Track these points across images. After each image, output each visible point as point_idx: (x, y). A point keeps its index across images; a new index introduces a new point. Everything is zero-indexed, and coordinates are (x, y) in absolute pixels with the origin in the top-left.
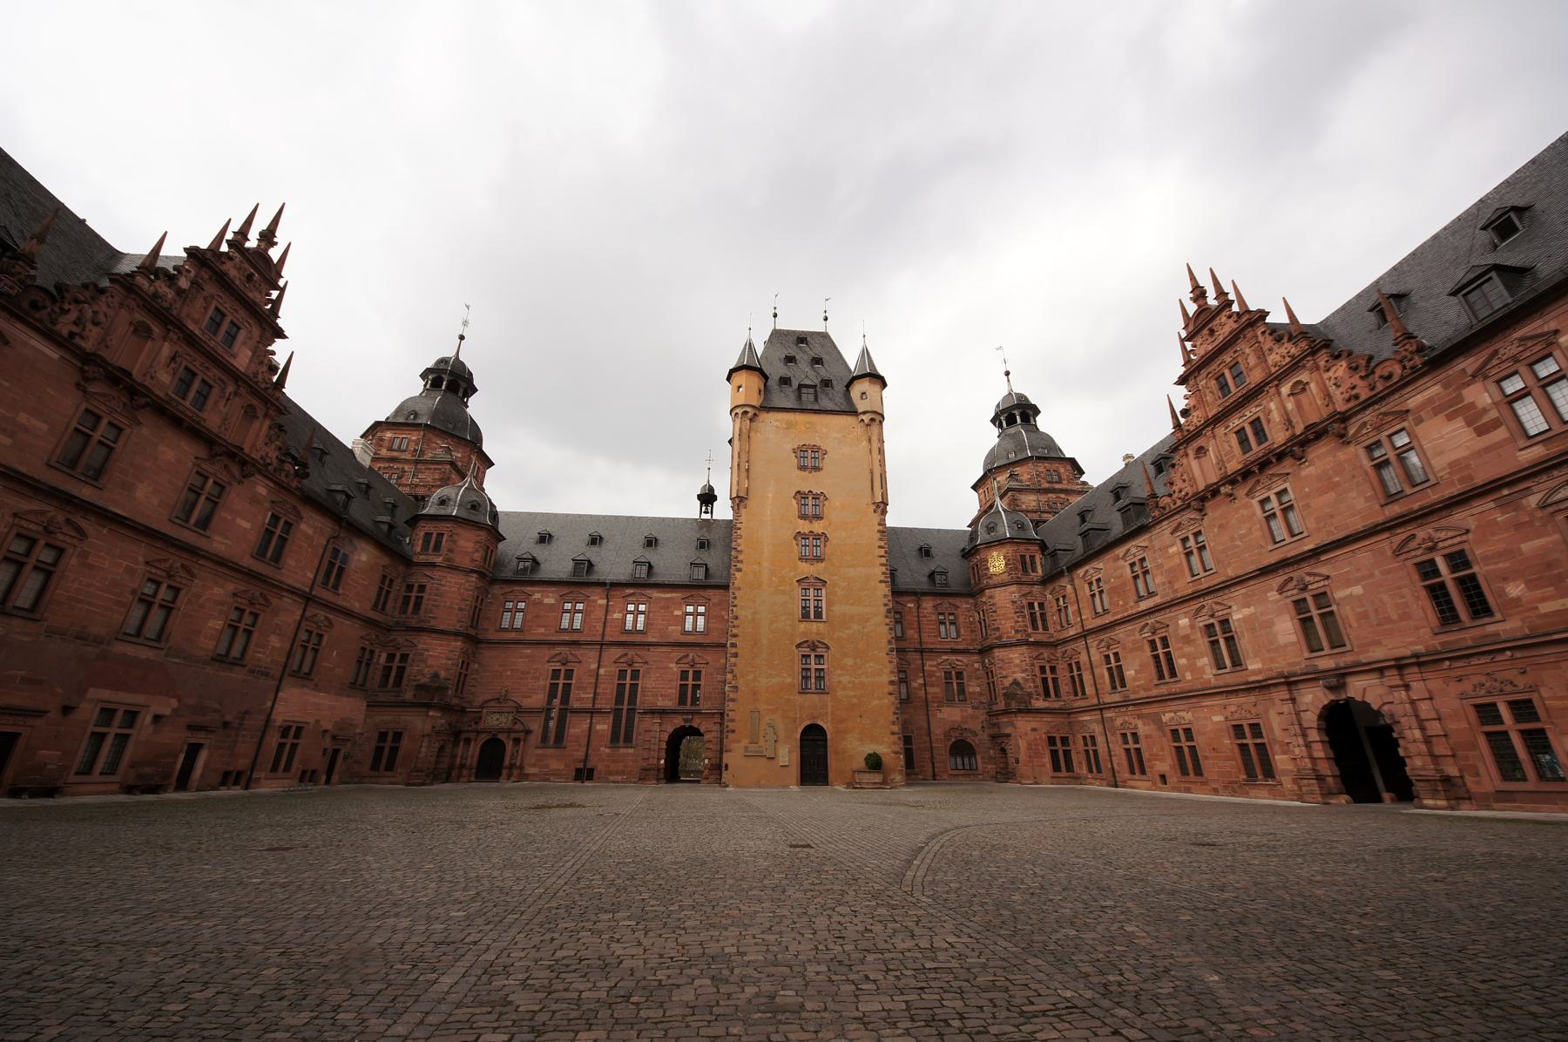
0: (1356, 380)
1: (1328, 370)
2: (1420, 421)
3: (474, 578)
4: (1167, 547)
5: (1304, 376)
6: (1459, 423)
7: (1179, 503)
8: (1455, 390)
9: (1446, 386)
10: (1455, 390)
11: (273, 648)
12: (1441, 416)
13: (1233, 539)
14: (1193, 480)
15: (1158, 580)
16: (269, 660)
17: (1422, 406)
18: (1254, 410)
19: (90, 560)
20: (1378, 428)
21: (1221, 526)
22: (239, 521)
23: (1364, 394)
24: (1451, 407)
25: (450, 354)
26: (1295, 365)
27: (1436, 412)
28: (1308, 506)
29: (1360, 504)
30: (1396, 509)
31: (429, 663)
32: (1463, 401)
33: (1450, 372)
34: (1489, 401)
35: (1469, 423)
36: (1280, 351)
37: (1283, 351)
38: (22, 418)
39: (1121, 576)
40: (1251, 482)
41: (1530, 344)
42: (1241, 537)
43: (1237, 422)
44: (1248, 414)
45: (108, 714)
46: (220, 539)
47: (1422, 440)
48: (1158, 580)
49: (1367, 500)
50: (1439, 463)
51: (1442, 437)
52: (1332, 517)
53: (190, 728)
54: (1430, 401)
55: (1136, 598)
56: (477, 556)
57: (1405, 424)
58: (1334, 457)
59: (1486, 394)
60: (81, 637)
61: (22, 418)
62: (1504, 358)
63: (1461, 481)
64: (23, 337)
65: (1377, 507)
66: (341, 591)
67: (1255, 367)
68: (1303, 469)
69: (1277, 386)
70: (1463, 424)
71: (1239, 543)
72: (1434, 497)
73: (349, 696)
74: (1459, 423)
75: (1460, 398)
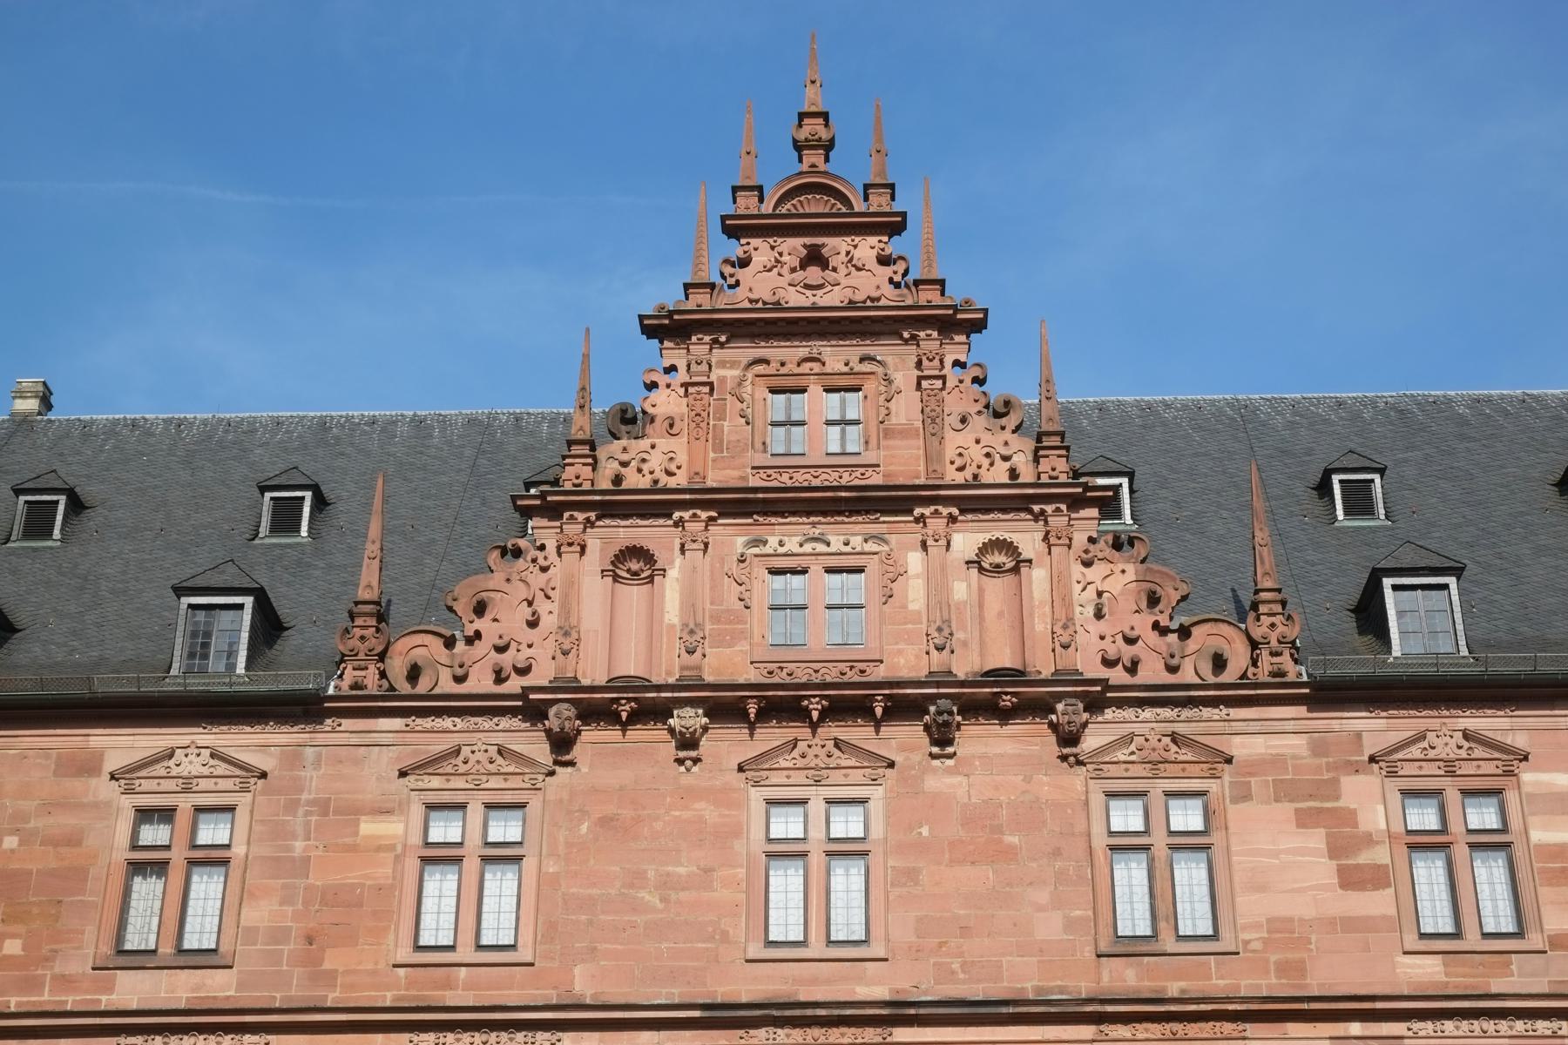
0: (1142, 624)
1: (1087, 564)
2: (1243, 795)
4: (356, 811)
5: (1027, 539)
6: (1316, 839)
7: (479, 682)
8: (1329, 767)
9: (1318, 749)
10: (1329, 767)
12: (1287, 809)
13: (636, 879)
14: (568, 633)
15: (257, 914)
17: (1257, 766)
18: (857, 541)
20: (1156, 765)
21: (605, 822)
23: (1154, 671)
24: (1311, 797)
26: (1016, 503)
27: (1283, 792)
28: (911, 875)
29: (1049, 927)
30: (1126, 977)
32: (1337, 798)
33: (1335, 725)
34: (1383, 826)
35: (1334, 851)
36: (987, 438)
37: (996, 441)
39: (73, 840)
40: (772, 735)
41: (1479, 752)
42: (666, 884)
43: (792, 545)
44: (836, 544)
47: (1233, 840)
48: (257, 914)
49: (1070, 925)
50: (1251, 908)
51: (1276, 854)
52: (965, 931)
54: (1277, 762)
55: (106, 949)
57: (1212, 786)
58: (1028, 780)
59: (1381, 808)
62: (1432, 754)
63: (1283, 968)
65: (1089, 953)
67: (905, 433)
68: (935, 770)
69: (952, 519)
70: (1323, 846)
71: (650, 897)
72: (1219, 980)
74: (1316, 839)
75: (1331, 789)
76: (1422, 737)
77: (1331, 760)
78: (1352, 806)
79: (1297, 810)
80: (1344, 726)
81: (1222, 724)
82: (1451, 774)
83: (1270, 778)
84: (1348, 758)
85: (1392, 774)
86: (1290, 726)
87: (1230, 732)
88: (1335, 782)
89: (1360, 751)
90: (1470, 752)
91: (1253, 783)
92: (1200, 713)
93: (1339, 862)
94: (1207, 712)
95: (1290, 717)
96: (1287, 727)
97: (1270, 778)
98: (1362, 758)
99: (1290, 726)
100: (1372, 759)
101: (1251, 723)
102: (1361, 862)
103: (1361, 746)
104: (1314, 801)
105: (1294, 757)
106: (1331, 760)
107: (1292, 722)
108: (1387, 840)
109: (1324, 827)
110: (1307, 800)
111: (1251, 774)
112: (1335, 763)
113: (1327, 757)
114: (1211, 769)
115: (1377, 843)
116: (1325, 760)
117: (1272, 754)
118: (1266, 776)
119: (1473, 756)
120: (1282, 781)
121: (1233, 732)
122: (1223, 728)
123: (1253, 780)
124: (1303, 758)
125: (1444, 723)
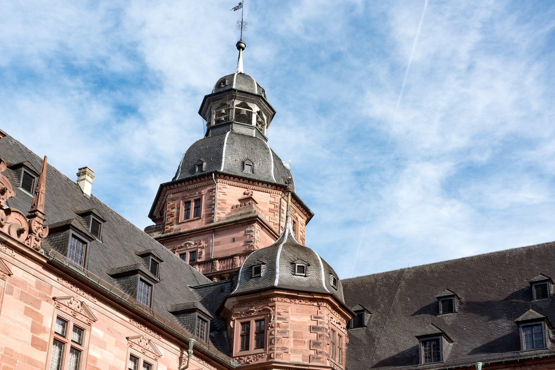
6: (28, 321)
8: (40, 295)
9: (38, 286)
10: (40, 295)
12: (22, 305)
17: (16, 282)
27: (23, 297)
34: (50, 327)
54: (24, 284)
74: (28, 321)
76: (69, 298)
77: (41, 292)
78: (43, 314)
79: (26, 307)
80: (49, 281)
81: (11, 258)
82: (74, 316)
83: (20, 290)
84: (46, 294)
85: (58, 307)
86: (33, 272)
87: (13, 263)
88: (40, 302)
89: (50, 294)
90: (81, 311)
91: (14, 289)
92: (5, 249)
93: (33, 335)
94: (9, 251)
95: (34, 268)
96: (32, 272)
97: (20, 290)
98: (50, 296)
99: (33, 272)
100: (54, 299)
101: (21, 264)
102: (40, 338)
103: (51, 291)
104: (32, 306)
105: (30, 285)
106: (41, 292)
107: (34, 271)
108: (50, 333)
109: (32, 318)
110: (30, 305)
111: (15, 285)
112: (42, 294)
113: (40, 290)
114: (3, 275)
115: (46, 332)
116: (39, 291)
117: (23, 280)
118: (19, 287)
119: (81, 313)
120: (24, 292)
121: (14, 264)
122: (11, 260)
123: (15, 287)
124: (32, 287)
125: (77, 296)
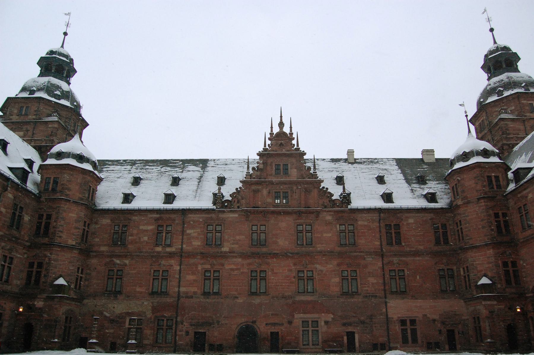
3: (482, 203)
11: (373, 284)
16: (373, 289)
19: (275, 271)
22: (325, 235)
25: (491, 46)
31: (479, 269)
38: (238, 237)
45: (305, 323)
46: (320, 245)
53: (344, 325)
56: (479, 187)
60: (284, 297)
61: (238, 237)
64: (228, 216)
66: (403, 244)
73: (444, 298)
